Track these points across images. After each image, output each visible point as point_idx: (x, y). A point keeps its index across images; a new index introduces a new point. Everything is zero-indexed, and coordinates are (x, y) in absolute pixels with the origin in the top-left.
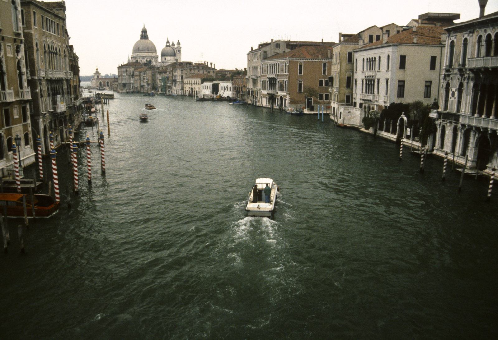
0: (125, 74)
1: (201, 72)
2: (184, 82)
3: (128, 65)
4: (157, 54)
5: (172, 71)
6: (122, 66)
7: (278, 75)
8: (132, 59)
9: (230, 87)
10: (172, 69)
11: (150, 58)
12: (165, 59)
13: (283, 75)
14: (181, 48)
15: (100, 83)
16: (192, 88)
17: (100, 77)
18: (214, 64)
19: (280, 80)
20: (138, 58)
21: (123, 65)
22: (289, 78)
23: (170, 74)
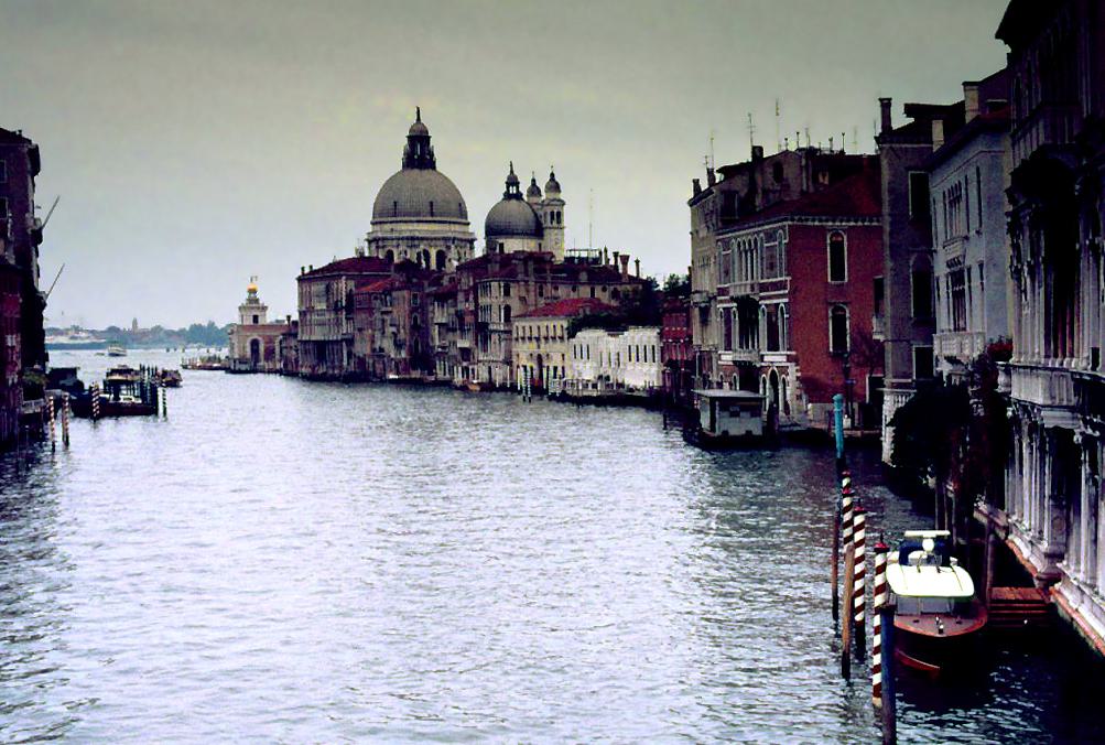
0: (323, 306)
1: (585, 292)
2: (515, 335)
3: (335, 270)
4: (471, 229)
5: (475, 289)
6: (313, 272)
7: (763, 288)
8: (369, 248)
9: (653, 347)
10: (474, 280)
11: (441, 243)
12: (502, 245)
13: (776, 286)
14: (563, 203)
15: (255, 343)
16: (539, 357)
17: (261, 321)
18: (637, 262)
19: (766, 305)
20: (395, 242)
21: (322, 270)
22: (791, 295)
23: (467, 300)
